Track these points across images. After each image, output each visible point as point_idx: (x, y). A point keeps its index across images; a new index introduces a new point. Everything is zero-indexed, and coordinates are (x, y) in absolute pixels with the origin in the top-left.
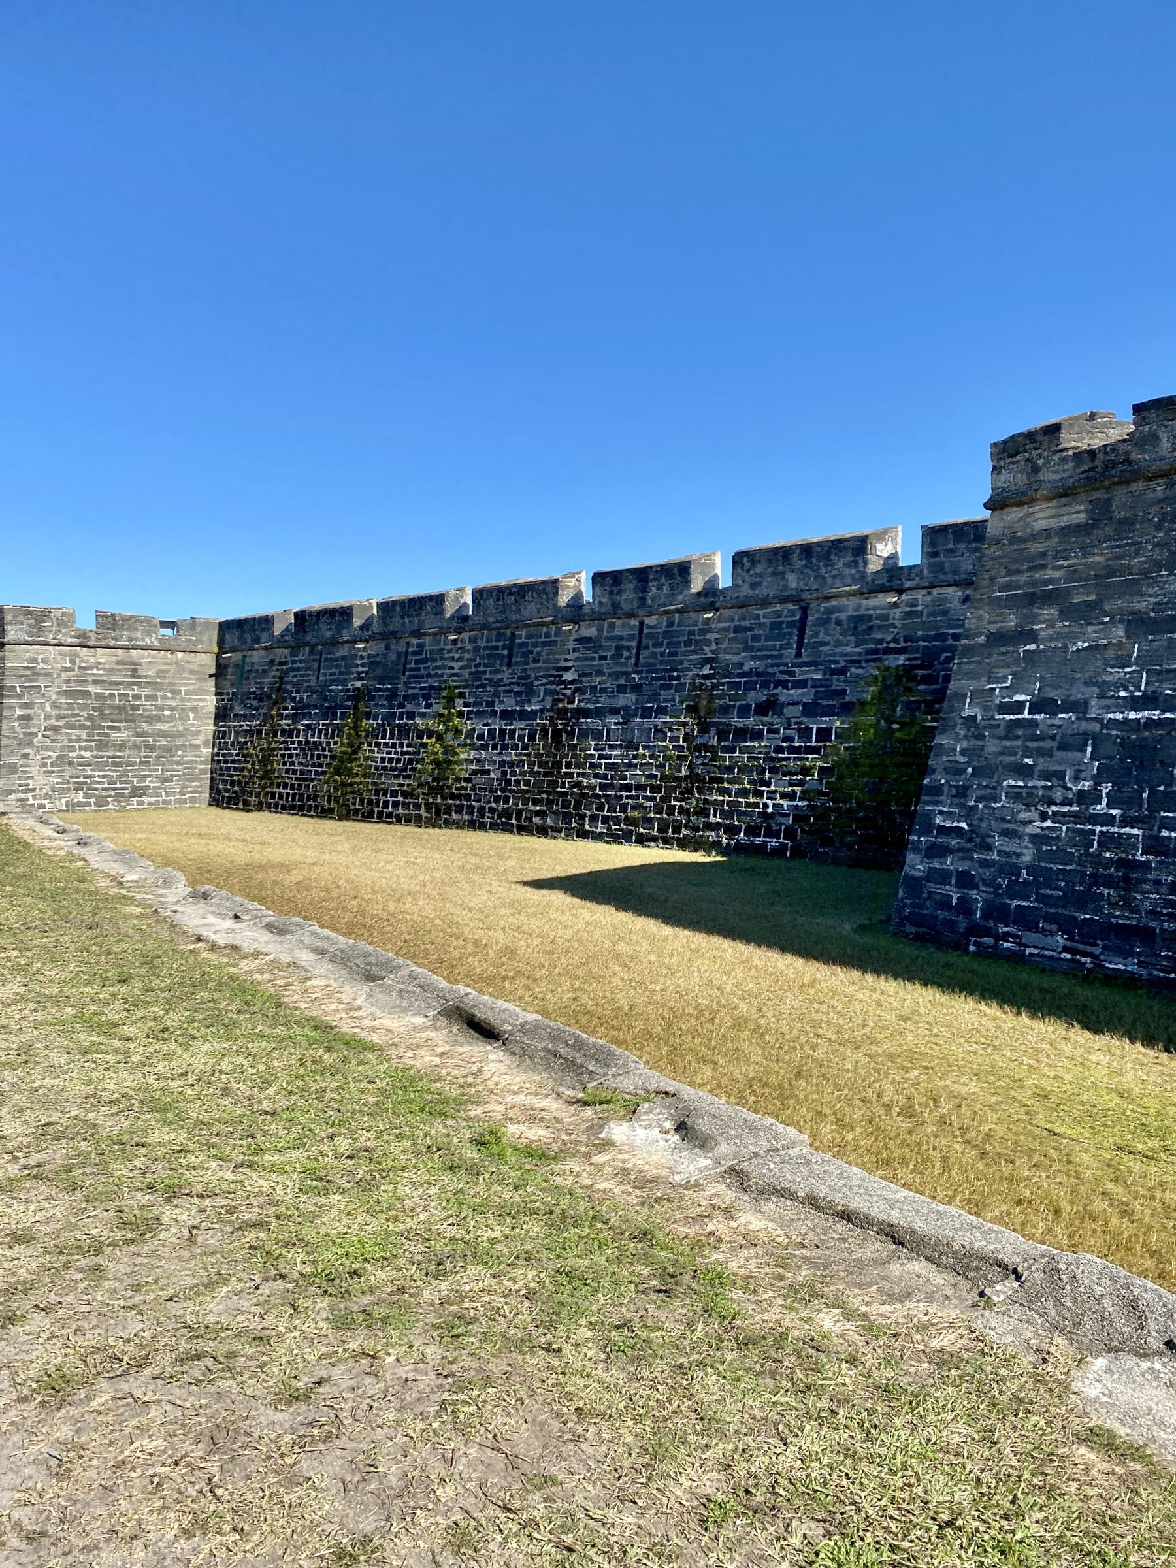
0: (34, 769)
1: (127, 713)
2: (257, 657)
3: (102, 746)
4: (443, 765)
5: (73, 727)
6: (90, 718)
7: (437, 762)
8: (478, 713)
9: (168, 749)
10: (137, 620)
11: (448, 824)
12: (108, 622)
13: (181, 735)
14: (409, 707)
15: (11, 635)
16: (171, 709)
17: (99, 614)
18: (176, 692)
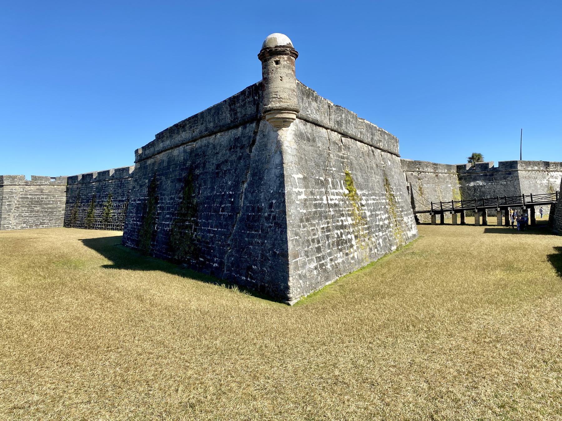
0: (11, 218)
1: (39, 203)
2: (75, 186)
3: (31, 212)
4: (107, 214)
5: (23, 207)
6: (28, 204)
7: (106, 213)
8: (115, 201)
9: (52, 212)
10: (43, 177)
11: (108, 229)
12: (34, 178)
13: (55, 208)
14: (103, 199)
15: (5, 183)
16: (53, 201)
17: (32, 176)
18: (54, 197)
